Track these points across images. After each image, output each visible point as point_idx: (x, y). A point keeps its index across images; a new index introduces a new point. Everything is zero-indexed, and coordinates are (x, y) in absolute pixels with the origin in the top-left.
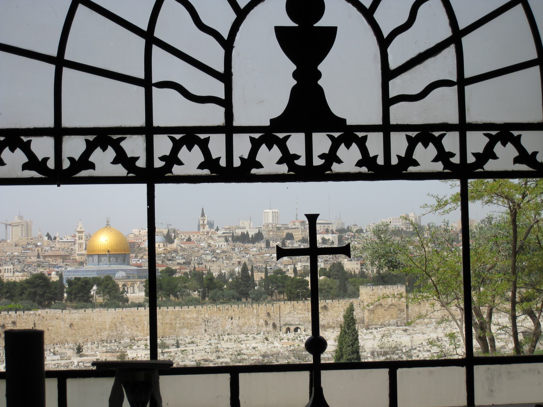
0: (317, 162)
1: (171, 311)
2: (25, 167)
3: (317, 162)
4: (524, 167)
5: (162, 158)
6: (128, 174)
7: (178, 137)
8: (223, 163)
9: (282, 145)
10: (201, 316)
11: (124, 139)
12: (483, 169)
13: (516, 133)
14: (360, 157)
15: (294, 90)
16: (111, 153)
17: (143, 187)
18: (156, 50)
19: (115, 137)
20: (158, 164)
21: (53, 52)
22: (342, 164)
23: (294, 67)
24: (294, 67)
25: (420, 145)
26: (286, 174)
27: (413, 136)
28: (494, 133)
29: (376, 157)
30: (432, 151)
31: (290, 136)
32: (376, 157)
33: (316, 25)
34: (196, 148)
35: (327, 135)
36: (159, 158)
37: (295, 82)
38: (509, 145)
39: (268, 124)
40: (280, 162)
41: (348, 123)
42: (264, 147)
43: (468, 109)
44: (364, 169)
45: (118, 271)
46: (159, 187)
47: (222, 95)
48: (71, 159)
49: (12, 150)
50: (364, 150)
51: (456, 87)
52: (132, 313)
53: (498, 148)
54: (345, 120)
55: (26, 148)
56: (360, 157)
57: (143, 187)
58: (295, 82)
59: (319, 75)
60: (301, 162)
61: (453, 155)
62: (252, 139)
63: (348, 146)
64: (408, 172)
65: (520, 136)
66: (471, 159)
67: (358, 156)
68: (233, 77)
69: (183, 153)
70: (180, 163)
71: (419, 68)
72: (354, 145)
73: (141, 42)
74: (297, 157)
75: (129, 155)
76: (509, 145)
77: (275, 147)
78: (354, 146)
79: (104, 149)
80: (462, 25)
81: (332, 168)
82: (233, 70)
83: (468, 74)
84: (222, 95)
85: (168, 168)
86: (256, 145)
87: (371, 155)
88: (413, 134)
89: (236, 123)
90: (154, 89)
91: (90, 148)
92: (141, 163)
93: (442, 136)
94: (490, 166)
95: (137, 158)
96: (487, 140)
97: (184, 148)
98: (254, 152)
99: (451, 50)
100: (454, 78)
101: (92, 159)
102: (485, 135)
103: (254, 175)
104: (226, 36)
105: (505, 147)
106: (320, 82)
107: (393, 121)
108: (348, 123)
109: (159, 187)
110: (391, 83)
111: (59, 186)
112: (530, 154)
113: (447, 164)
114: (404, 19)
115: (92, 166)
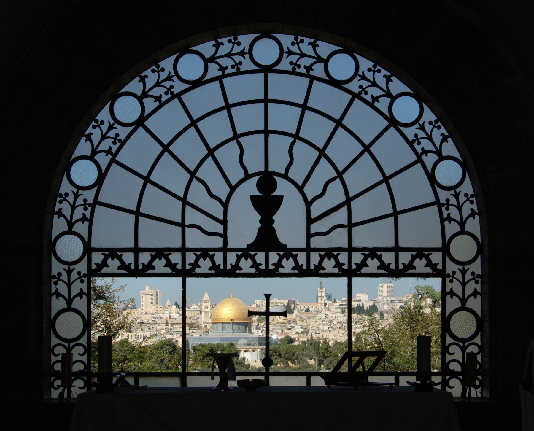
0: (271, 267)
2: (119, 268)
3: (271, 267)
4: (383, 271)
5: (190, 264)
6: (172, 272)
7: (198, 253)
8: (222, 267)
9: (253, 258)
11: (171, 254)
12: (360, 272)
13: (379, 253)
14: (294, 265)
15: (260, 230)
16: (163, 261)
17: (180, 279)
18: (187, 207)
19: (166, 253)
20: (188, 267)
21: (134, 208)
22: (284, 269)
23: (260, 217)
24: (260, 217)
25: (326, 259)
26: (255, 274)
27: (323, 254)
28: (367, 253)
29: (302, 265)
30: (333, 262)
31: (257, 253)
32: (302, 265)
33: (272, 195)
34: (208, 259)
35: (277, 253)
36: (188, 264)
37: (260, 225)
38: (375, 259)
39: (245, 247)
40: (251, 267)
41: (288, 247)
42: (243, 259)
43: (353, 240)
44: (296, 271)
46: (188, 279)
47: (222, 232)
48: (143, 264)
49: (113, 259)
50: (296, 262)
51: (347, 228)
53: (369, 261)
54: (286, 246)
55: (120, 258)
56: (294, 265)
57: (180, 279)
58: (260, 225)
59: (273, 221)
60: (263, 267)
61: (344, 264)
62: (237, 255)
63: (288, 259)
64: (319, 273)
65: (381, 255)
66: (354, 267)
67: (293, 265)
68: (228, 222)
69: (201, 262)
70: (199, 267)
71: (326, 218)
72: (291, 259)
73: (180, 203)
74: (261, 265)
75: (173, 262)
76: (375, 259)
77: (249, 259)
78: (291, 259)
79: (160, 259)
80: (351, 195)
81: (279, 270)
82: (228, 219)
83: (353, 221)
84: (222, 232)
85: (193, 269)
86: (239, 258)
87: (300, 264)
88: (323, 253)
89: (229, 247)
90: (186, 228)
91: (153, 258)
92: (179, 267)
93: (338, 254)
94: (364, 270)
95: (177, 264)
96: (363, 257)
97: (202, 259)
98: (238, 262)
99: (345, 209)
100: (346, 224)
101: (154, 264)
102: (362, 254)
103: (238, 274)
104: (224, 201)
105: (373, 260)
106: (274, 225)
107: (312, 246)
108: (288, 247)
109: (188, 279)
110: (312, 226)
111: (136, 278)
112: (386, 264)
113: (341, 269)
114: (320, 192)
115: (154, 268)
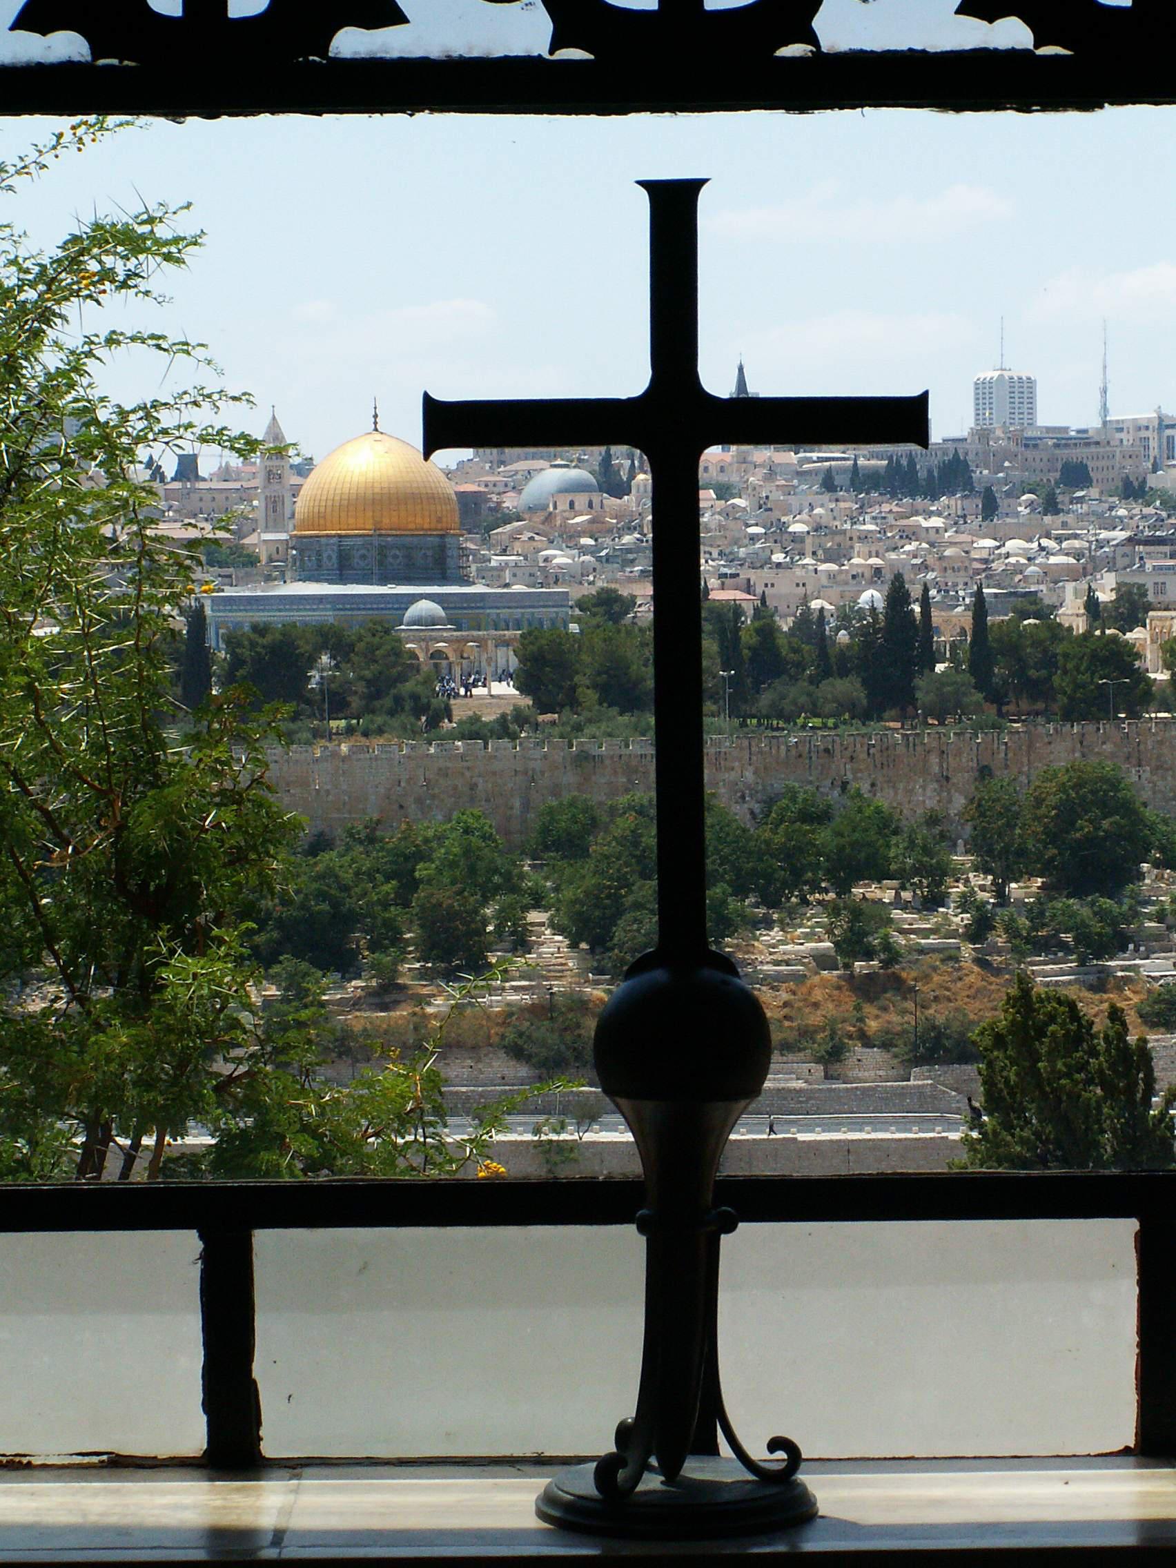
1: (612, 757)
10: (733, 776)
45: (415, 598)
52: (465, 764)
